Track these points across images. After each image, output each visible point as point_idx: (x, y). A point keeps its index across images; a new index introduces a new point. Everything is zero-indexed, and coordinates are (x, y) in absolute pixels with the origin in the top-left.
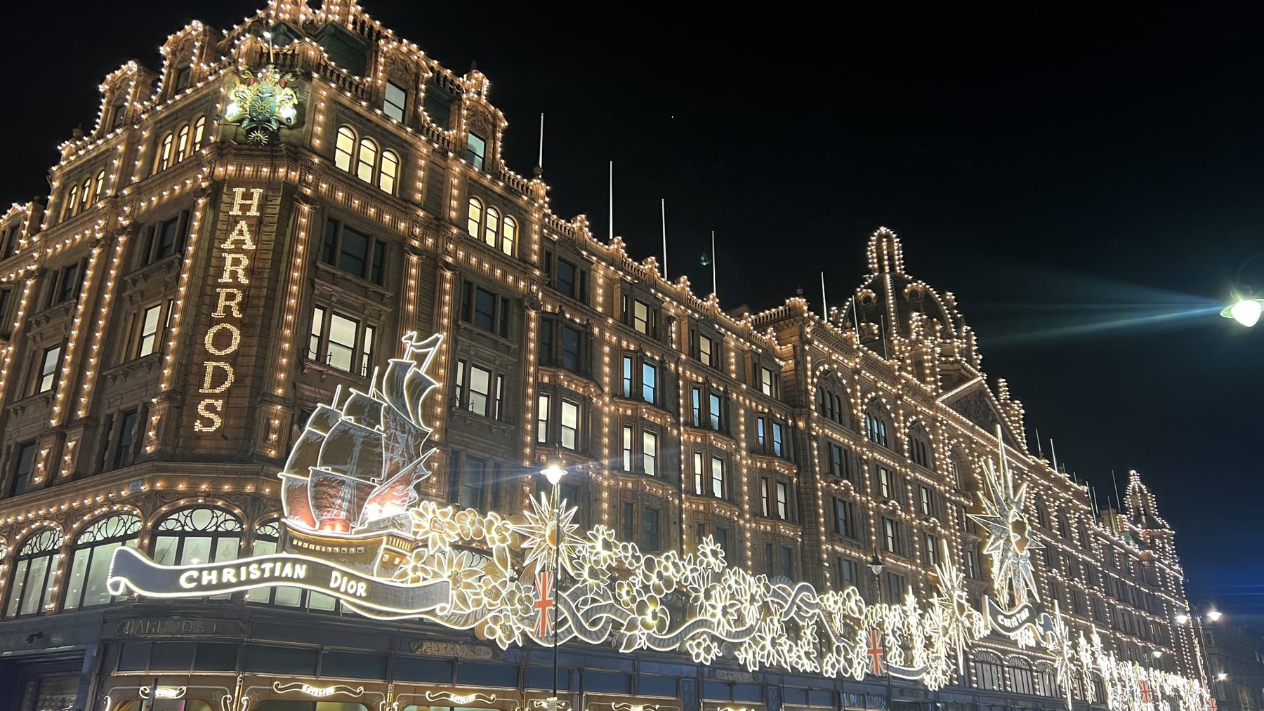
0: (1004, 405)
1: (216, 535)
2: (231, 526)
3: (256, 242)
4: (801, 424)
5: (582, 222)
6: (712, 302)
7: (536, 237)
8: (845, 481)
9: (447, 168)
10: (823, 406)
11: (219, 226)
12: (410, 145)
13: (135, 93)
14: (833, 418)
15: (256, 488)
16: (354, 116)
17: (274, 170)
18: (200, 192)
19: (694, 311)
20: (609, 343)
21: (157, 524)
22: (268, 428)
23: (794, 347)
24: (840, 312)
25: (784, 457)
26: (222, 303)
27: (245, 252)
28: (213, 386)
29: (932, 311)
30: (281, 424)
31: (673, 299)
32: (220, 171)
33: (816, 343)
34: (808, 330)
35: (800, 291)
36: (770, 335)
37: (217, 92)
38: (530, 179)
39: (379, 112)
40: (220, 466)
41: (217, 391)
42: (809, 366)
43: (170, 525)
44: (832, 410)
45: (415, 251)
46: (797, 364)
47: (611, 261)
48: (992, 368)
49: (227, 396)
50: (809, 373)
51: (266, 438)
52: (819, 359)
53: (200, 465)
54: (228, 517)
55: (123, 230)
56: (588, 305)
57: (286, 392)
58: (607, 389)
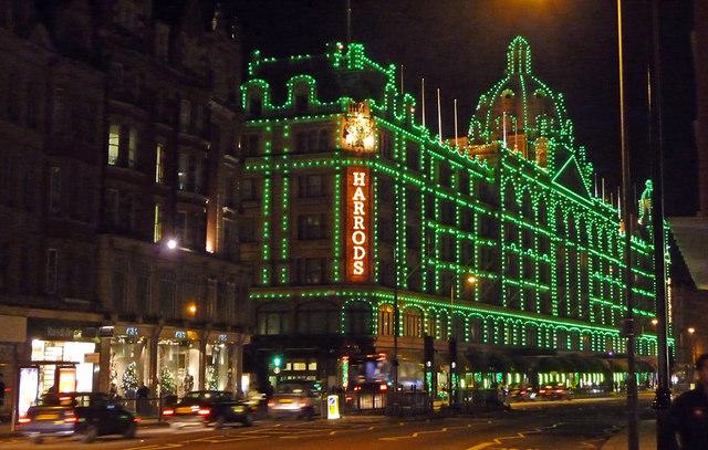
0: (581, 166)
11: (347, 189)
26: (356, 223)
29: (546, 107)
41: (362, 257)
48: (576, 146)
52: (507, 173)
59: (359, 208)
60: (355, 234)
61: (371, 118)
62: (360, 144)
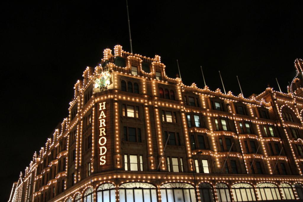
1: (110, 190)
2: (113, 187)
3: (106, 115)
4: (279, 125)
5: (194, 85)
6: (241, 96)
7: (180, 93)
8: (299, 139)
9: (151, 83)
10: (286, 117)
12: (140, 80)
13: (80, 87)
14: (290, 121)
15: (117, 176)
16: (124, 77)
17: (107, 96)
18: (93, 107)
19: (235, 100)
20: (209, 116)
21: (97, 189)
22: (117, 161)
23: (271, 102)
24: (290, 87)
25: (276, 136)
26: (101, 132)
27: (104, 118)
28: (103, 153)
30: (120, 159)
31: (227, 98)
32: (96, 100)
33: (278, 99)
34: (274, 96)
35: (268, 86)
36: (262, 101)
37: (93, 82)
38: (175, 78)
39: (130, 74)
40: (108, 172)
41: (104, 153)
42: (277, 107)
43: (100, 189)
44: (289, 118)
45: (146, 106)
46: (273, 107)
47: (205, 93)
49: (106, 155)
50: (278, 109)
51: (117, 163)
52: (280, 104)
53: (103, 173)
54: (112, 185)
55: (82, 120)
56: (201, 107)
57: (119, 151)
58: (211, 129)
59: (102, 123)
60: (100, 140)
61: (111, 72)
62: (103, 87)
